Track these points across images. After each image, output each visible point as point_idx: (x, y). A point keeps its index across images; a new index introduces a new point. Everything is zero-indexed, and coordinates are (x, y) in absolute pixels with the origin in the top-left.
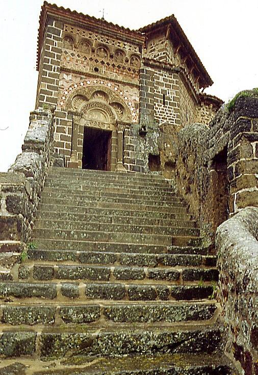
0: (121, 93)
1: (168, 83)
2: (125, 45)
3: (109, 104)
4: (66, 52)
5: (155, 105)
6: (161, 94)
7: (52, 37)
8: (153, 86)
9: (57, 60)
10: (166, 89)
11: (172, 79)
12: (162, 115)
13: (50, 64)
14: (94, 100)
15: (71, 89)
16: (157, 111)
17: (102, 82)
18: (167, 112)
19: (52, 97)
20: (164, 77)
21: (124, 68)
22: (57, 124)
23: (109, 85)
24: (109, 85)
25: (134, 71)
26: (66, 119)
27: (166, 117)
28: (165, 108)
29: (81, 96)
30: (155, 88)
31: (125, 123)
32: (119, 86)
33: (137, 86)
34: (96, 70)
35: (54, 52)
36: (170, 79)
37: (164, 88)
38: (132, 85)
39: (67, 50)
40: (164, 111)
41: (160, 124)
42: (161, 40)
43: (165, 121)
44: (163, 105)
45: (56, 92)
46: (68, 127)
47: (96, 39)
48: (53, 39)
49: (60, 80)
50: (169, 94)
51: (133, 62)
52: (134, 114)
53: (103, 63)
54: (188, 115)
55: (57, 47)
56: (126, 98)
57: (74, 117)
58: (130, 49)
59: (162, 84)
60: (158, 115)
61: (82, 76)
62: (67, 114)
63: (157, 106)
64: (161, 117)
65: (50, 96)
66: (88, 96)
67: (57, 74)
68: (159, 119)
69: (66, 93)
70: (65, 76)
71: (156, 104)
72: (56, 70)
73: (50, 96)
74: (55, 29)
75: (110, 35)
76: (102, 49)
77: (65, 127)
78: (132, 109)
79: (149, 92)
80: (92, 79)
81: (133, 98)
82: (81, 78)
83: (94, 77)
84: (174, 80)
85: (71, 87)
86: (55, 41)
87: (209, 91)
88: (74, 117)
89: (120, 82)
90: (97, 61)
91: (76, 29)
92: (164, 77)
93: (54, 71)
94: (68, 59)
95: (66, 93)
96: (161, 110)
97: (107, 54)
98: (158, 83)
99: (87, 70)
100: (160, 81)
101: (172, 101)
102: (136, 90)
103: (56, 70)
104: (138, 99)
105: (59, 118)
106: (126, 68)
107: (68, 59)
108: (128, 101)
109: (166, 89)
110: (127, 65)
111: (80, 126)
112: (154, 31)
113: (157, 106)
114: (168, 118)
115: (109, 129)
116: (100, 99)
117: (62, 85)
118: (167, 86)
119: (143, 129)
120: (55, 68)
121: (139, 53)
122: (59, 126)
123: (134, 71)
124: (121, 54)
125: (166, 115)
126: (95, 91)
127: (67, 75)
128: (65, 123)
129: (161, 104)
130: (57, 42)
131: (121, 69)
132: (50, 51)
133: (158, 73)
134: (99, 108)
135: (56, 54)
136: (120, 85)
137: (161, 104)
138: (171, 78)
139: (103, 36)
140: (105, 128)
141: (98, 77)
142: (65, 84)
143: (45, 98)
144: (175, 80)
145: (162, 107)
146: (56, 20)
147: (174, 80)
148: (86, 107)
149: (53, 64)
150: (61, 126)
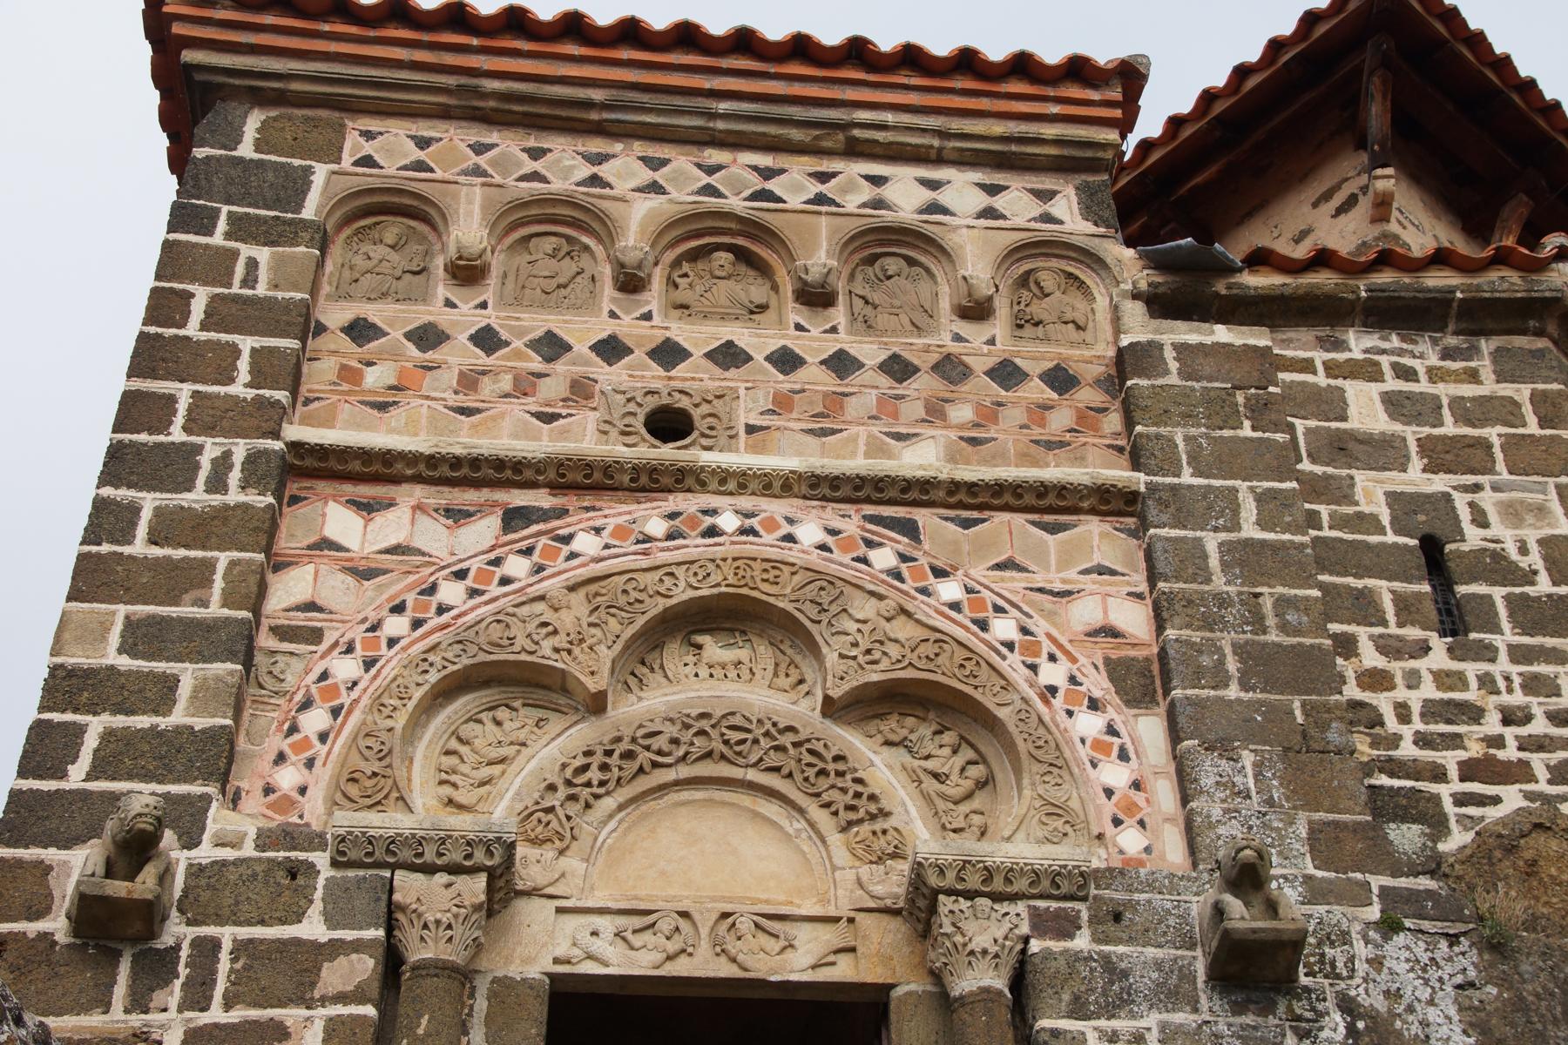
0: (950, 590)
1: (1449, 428)
2: (933, 185)
3: (831, 708)
4: (360, 331)
5: (1347, 646)
6: (1391, 538)
7: (222, 225)
8: (1285, 469)
9: (250, 393)
10: (1439, 483)
11: (1489, 386)
12: (1455, 741)
13: (177, 434)
15: (396, 625)
16: (1383, 702)
17: (728, 522)
18: (1518, 698)
19: (164, 722)
20: (1392, 384)
21: (951, 368)
22: (197, 997)
23: (810, 532)
24: (810, 532)
25: (1061, 380)
26: (313, 928)
27: (1510, 753)
28: (1472, 669)
29: (513, 681)
30: (1317, 488)
31: (1009, 875)
32: (910, 529)
33: (1112, 503)
35: (224, 337)
36: (1468, 390)
37: (1416, 478)
38: (1052, 504)
39: (375, 313)
40: (1472, 695)
41: (1457, 840)
42: (1327, 196)
43: (1512, 798)
44: (1439, 644)
45: (226, 669)
46: (321, 1012)
47: (643, 189)
48: (228, 236)
49: (279, 565)
50: (1481, 520)
51: (1038, 309)
52: (1116, 775)
53: (729, 356)
55: (261, 290)
56: (1004, 628)
57: (409, 886)
58: (989, 213)
59: (1384, 452)
60: (1407, 750)
61: (520, 498)
62: (326, 872)
63: (1371, 658)
64: (1450, 760)
65: (142, 721)
66: (593, 668)
67: (244, 507)
68: (1434, 788)
69: (345, 668)
70: (339, 521)
71: (1363, 633)
72: (235, 477)
73: (142, 721)
74: (261, 163)
75: (796, 134)
76: (724, 257)
77: (291, 1015)
78: (1089, 724)
79: (1250, 530)
80: (616, 512)
81: (1085, 613)
82: (514, 518)
83: (649, 482)
84: (1506, 390)
85: (399, 609)
86: (246, 250)
88: (409, 886)
89: (919, 491)
90: (668, 354)
91: (456, 138)
92: (1392, 384)
93: (217, 483)
94: (376, 377)
95: (345, 668)
96: (1429, 690)
97: (775, 288)
98: (1343, 448)
99: (584, 437)
100: (1353, 423)
101: (1544, 585)
102: (1097, 537)
103: (235, 477)
104: (1134, 620)
105: (227, 934)
106: (979, 364)
107: (376, 377)
108: (1032, 649)
109: (1439, 483)
110: (983, 344)
111: (504, 988)
113: (1371, 658)
114: (1538, 761)
115: (843, 971)
117: (311, 606)
118: (1440, 456)
119: (1235, 905)
120: (223, 464)
121: (1090, 228)
122: (216, 1014)
123: (1061, 380)
124: (911, 262)
125: (1510, 733)
126: (658, 606)
127: (367, 508)
128: (295, 972)
129: (1413, 633)
130: (263, 254)
131: (924, 384)
132: (192, 330)
133: (1319, 357)
134: (722, 758)
135: (247, 343)
136: (923, 517)
137: (1413, 633)
138: (1473, 376)
139: (714, 156)
140: (799, 961)
141: (684, 479)
142: (336, 589)
143: (91, 742)
144: (1522, 392)
145: (1439, 657)
146: (260, 98)
147: (1506, 390)
149: (210, 430)
150: (236, 1015)
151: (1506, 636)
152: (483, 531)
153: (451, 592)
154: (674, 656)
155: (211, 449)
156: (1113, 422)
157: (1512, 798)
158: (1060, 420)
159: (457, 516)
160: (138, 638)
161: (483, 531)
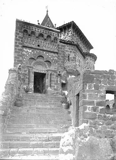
14: (38, 60)
23: (44, 53)
34: (39, 46)
43: (69, 68)
54: (80, 64)
66: (36, 58)
70: (25, 49)
87: (91, 51)
112: (63, 29)
116: (40, 60)
127: (26, 49)
133: (67, 46)
134: (40, 63)
140: (43, 72)
148: (35, 64)
151: (71, 61)
152: (31, 51)
153: (30, 54)
154: (39, 57)
155: (19, 45)
156: (57, 48)
157: (69, 68)
158: (55, 48)
159: (30, 50)
160: (18, 55)
161: (31, 51)
